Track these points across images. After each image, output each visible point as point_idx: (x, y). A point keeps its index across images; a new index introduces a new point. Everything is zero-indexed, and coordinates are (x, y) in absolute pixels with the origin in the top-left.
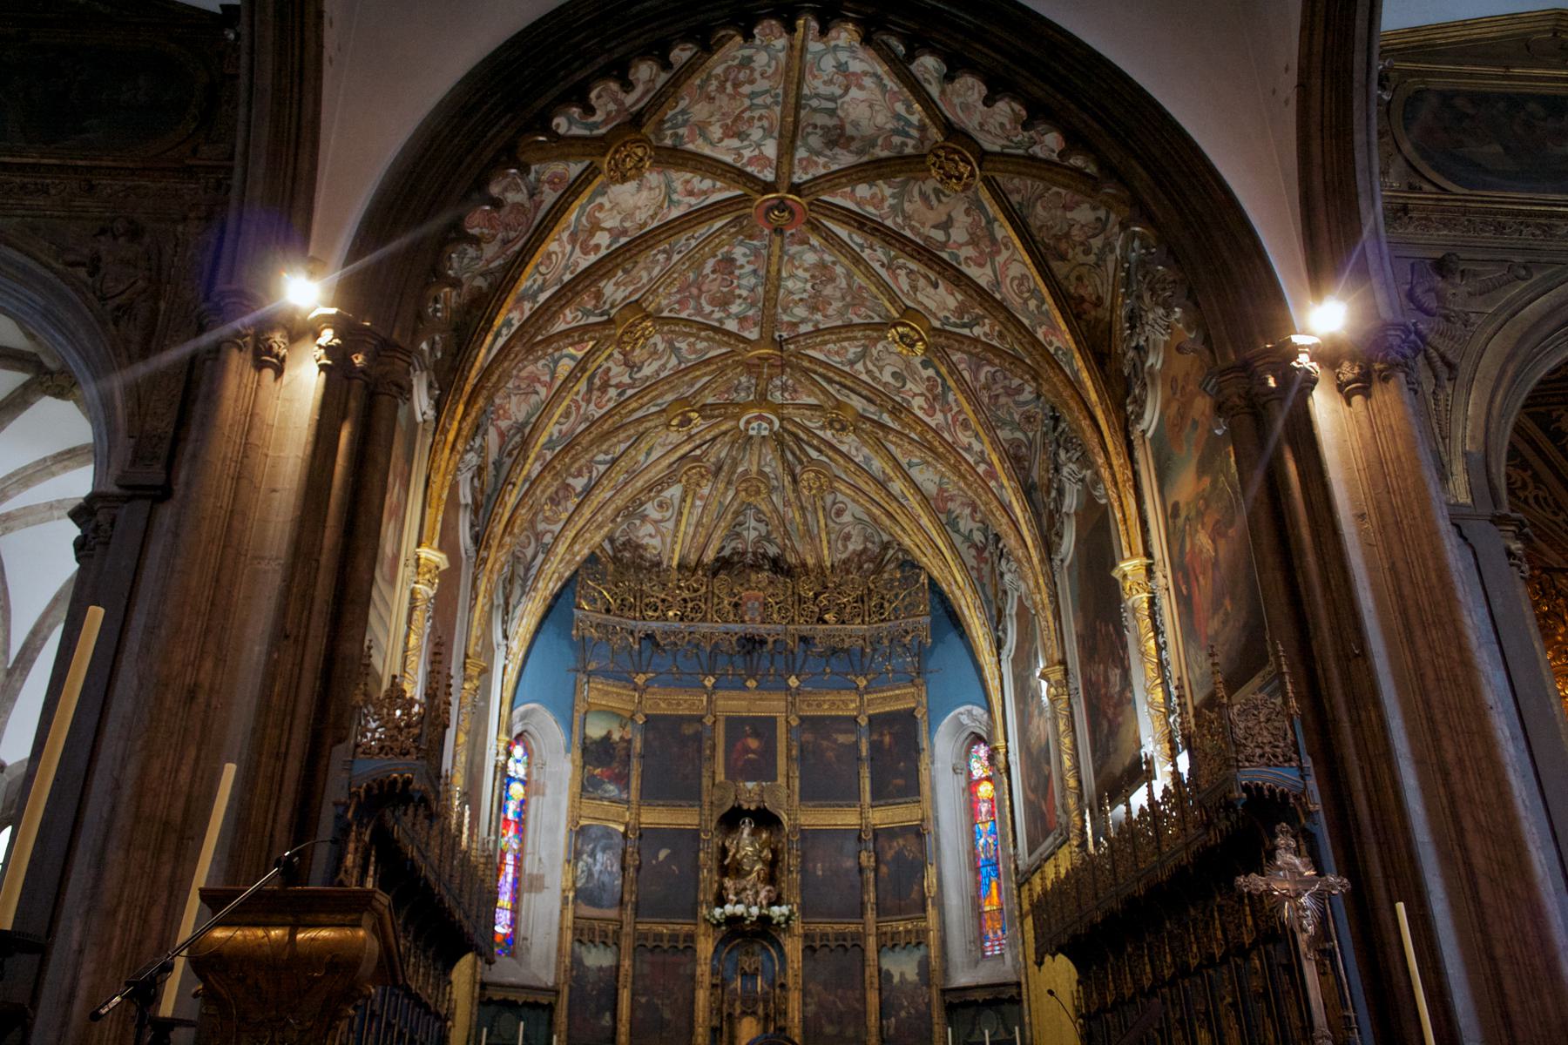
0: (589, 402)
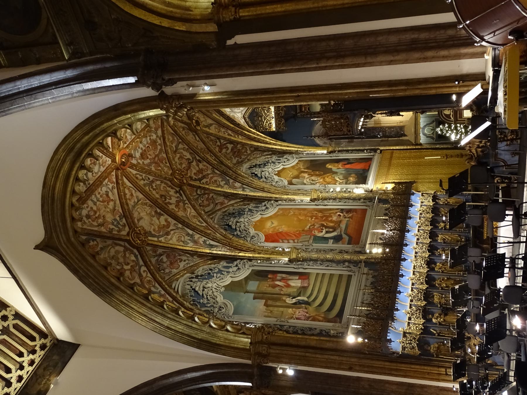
0: (208, 174)
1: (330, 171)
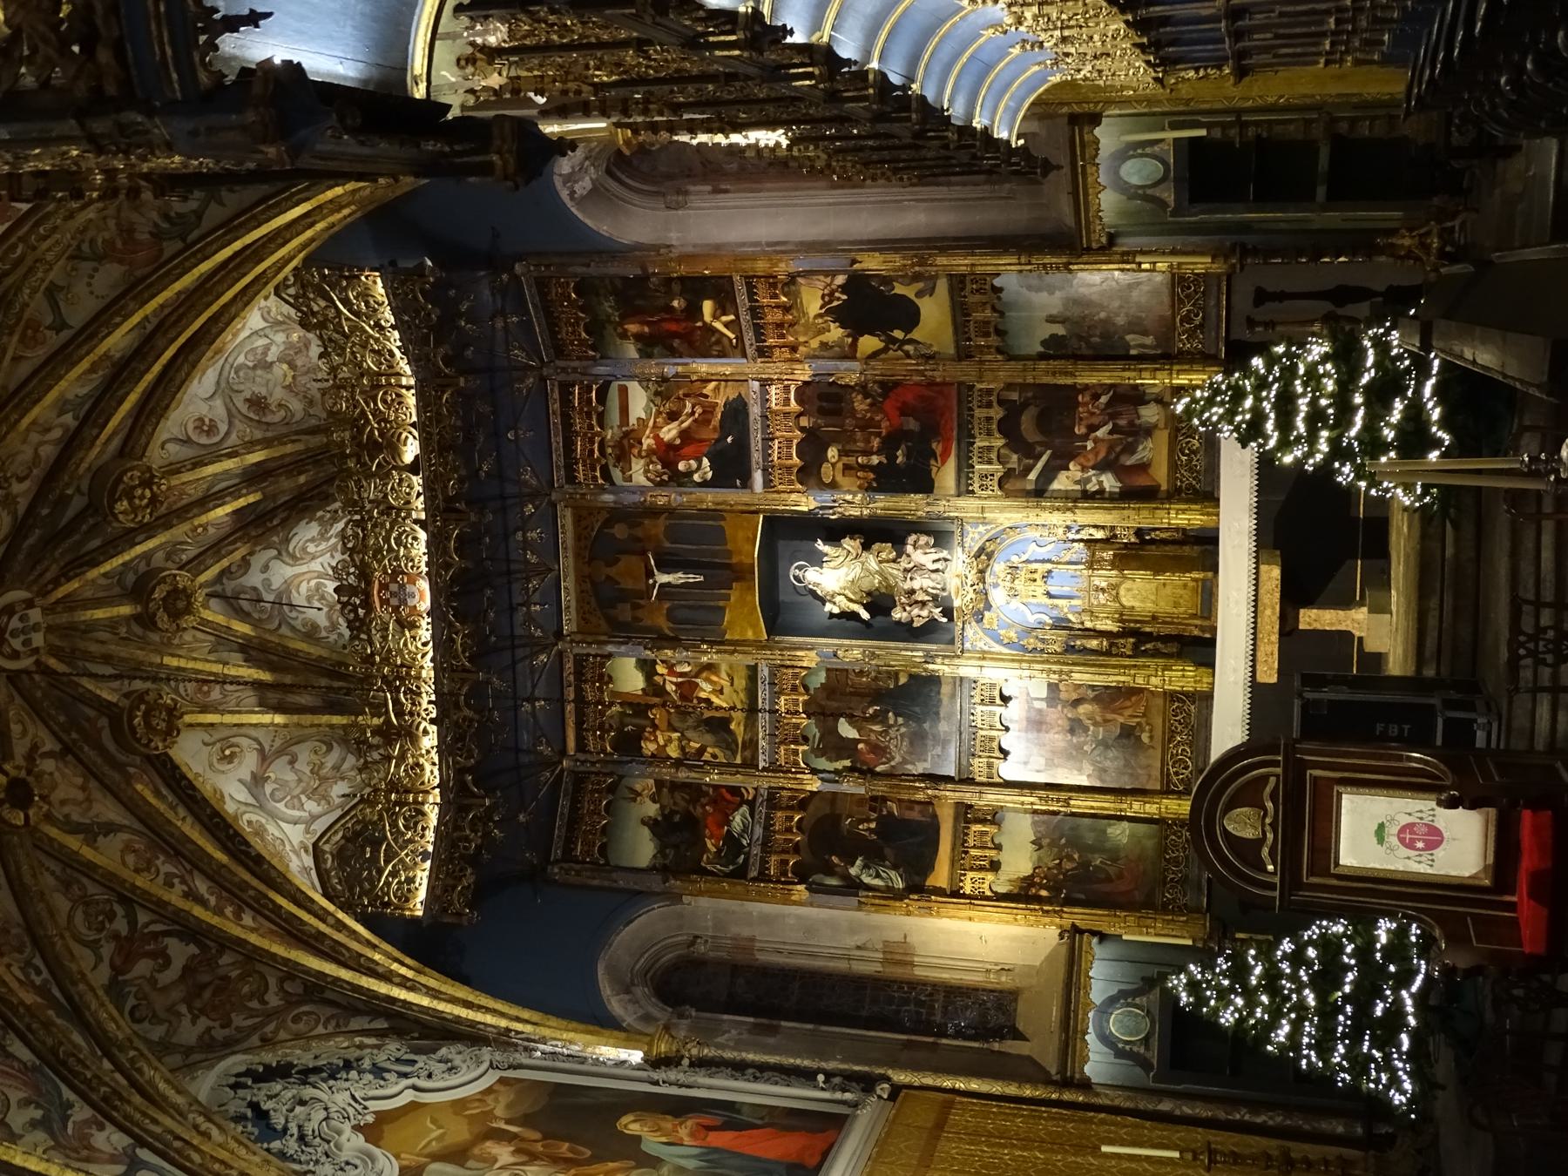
1: (631, 1149)
